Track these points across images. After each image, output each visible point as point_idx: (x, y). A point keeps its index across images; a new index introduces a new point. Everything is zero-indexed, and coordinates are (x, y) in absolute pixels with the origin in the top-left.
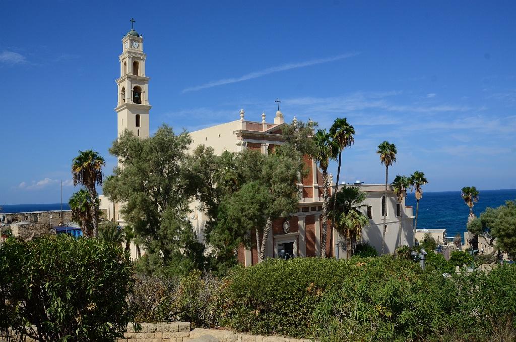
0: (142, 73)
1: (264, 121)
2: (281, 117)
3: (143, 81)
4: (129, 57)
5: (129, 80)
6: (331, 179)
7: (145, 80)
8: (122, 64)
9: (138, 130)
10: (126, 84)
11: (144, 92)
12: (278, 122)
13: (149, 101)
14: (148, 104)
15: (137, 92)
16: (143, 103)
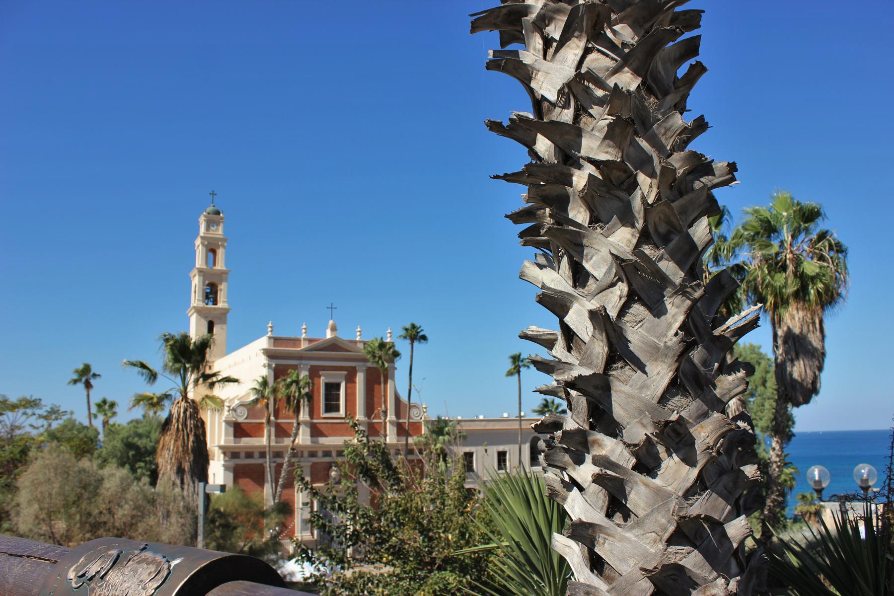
0: (220, 266)
1: (304, 335)
2: (334, 329)
3: (222, 275)
4: (203, 244)
5: (199, 276)
6: (425, 410)
10: (196, 281)
11: (221, 290)
12: (329, 335)
14: (226, 305)
15: (211, 293)
16: (220, 305)
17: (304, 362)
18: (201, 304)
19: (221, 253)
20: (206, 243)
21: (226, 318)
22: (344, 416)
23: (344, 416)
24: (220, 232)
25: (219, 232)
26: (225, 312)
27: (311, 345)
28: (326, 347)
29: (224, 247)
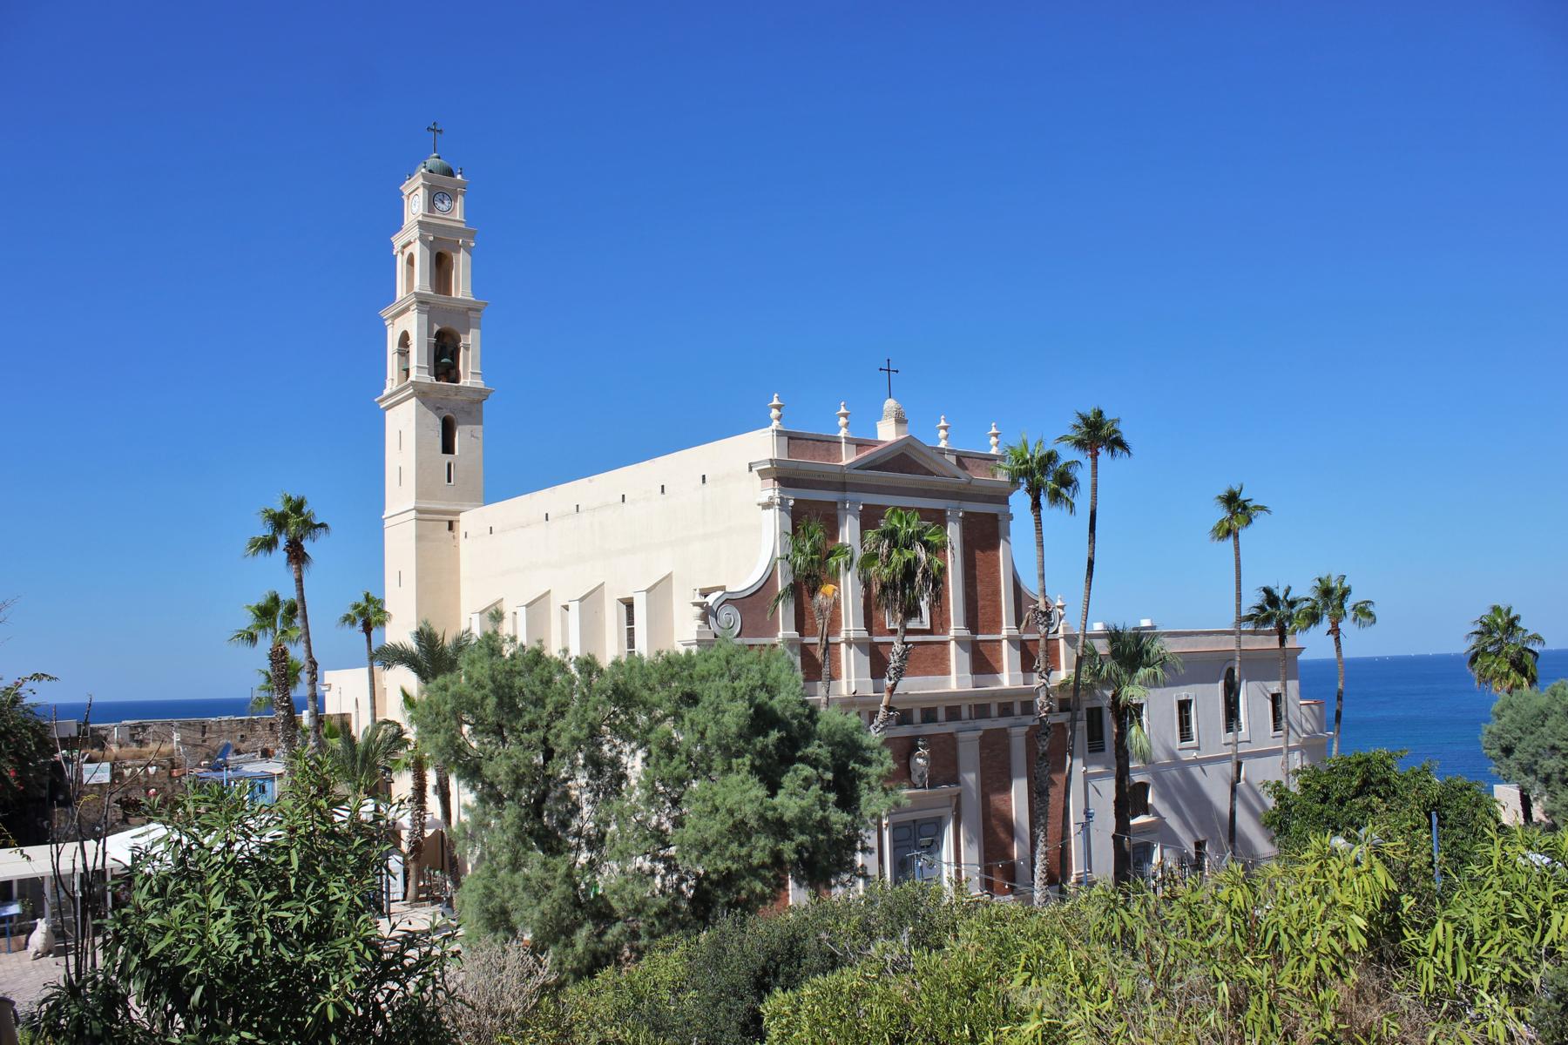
0: (461, 288)
2: (900, 420)
3: (467, 314)
4: (422, 239)
5: (420, 312)
7: (470, 309)
8: (401, 262)
9: (449, 465)
10: (411, 323)
11: (467, 348)
12: (887, 432)
13: (485, 372)
14: (479, 383)
16: (465, 381)
17: (849, 495)
18: (428, 379)
19: (461, 264)
20: (431, 238)
21: (480, 412)
22: (928, 627)
23: (928, 627)
24: (458, 214)
25: (456, 213)
26: (477, 399)
27: (861, 455)
28: (888, 462)
29: (469, 250)
